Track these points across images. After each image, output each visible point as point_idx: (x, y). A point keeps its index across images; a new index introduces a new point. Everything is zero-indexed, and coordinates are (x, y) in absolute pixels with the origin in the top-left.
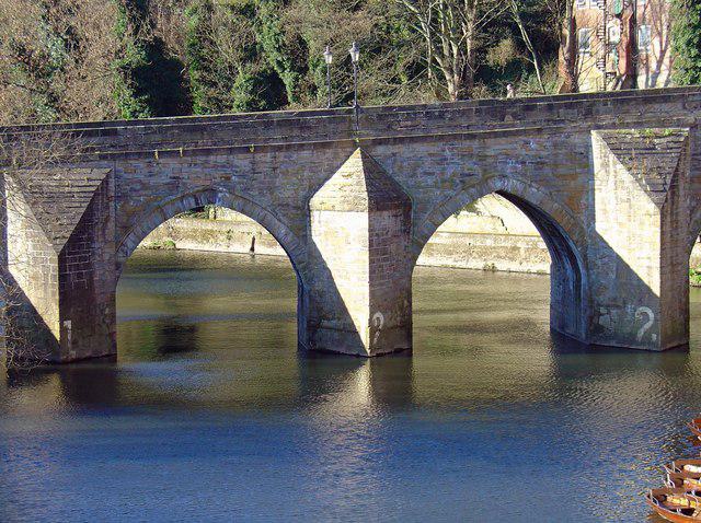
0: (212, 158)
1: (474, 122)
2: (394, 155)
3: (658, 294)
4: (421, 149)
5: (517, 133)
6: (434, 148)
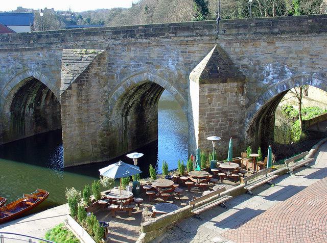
5: (33, 49)
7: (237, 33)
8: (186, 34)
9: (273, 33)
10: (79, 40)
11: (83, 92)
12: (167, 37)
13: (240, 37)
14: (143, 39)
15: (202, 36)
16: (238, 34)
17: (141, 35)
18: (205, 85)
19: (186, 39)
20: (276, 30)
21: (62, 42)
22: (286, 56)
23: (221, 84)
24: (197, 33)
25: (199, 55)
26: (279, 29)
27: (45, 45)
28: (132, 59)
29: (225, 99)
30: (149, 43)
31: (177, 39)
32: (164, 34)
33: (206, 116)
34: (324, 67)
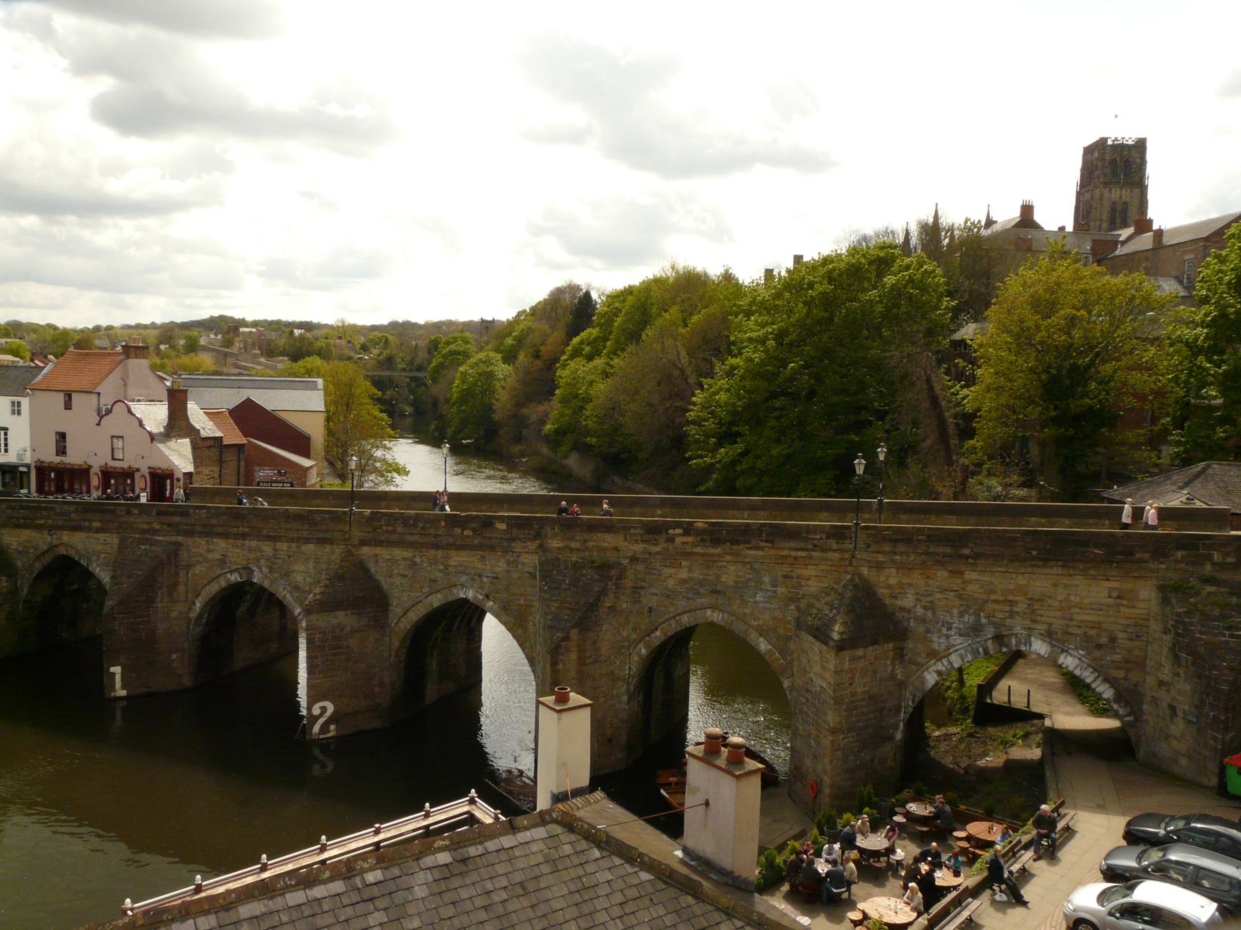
0: (247, 542)
1: (440, 532)
2: (376, 555)
3: (905, 820)
4: (398, 553)
6: (407, 554)
7: (892, 549)
8: (792, 544)
9: (961, 556)
10: (572, 539)
11: (589, 642)
12: (757, 548)
13: (898, 557)
14: (707, 547)
15: (825, 551)
16: (895, 553)
17: (703, 540)
18: (846, 652)
19: (793, 553)
20: (966, 551)
21: (535, 538)
22: (984, 597)
23: (870, 648)
24: (815, 546)
25: (819, 584)
26: (972, 548)
27: (498, 541)
28: (683, 581)
29: (875, 672)
30: (719, 555)
31: (772, 552)
32: (749, 543)
33: (845, 706)
34: (1054, 621)
